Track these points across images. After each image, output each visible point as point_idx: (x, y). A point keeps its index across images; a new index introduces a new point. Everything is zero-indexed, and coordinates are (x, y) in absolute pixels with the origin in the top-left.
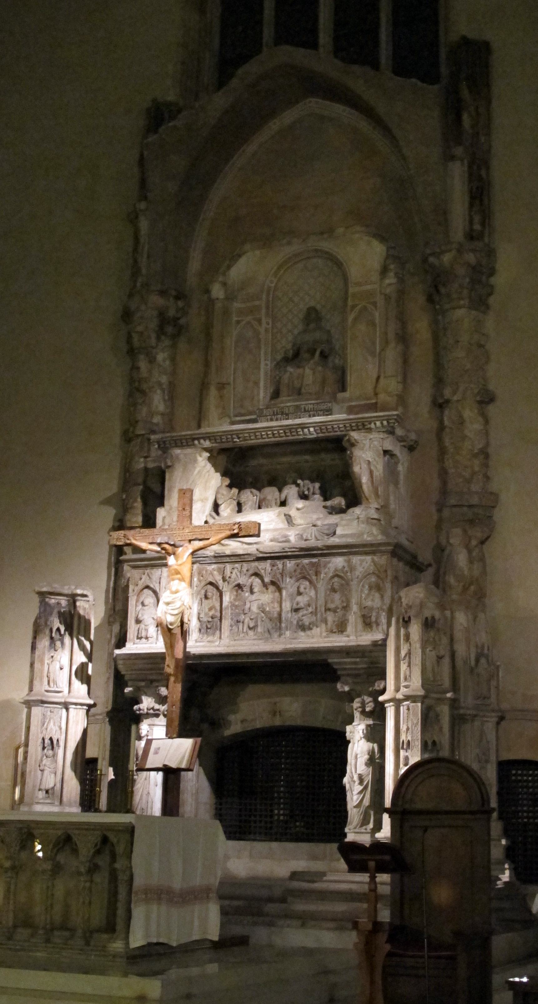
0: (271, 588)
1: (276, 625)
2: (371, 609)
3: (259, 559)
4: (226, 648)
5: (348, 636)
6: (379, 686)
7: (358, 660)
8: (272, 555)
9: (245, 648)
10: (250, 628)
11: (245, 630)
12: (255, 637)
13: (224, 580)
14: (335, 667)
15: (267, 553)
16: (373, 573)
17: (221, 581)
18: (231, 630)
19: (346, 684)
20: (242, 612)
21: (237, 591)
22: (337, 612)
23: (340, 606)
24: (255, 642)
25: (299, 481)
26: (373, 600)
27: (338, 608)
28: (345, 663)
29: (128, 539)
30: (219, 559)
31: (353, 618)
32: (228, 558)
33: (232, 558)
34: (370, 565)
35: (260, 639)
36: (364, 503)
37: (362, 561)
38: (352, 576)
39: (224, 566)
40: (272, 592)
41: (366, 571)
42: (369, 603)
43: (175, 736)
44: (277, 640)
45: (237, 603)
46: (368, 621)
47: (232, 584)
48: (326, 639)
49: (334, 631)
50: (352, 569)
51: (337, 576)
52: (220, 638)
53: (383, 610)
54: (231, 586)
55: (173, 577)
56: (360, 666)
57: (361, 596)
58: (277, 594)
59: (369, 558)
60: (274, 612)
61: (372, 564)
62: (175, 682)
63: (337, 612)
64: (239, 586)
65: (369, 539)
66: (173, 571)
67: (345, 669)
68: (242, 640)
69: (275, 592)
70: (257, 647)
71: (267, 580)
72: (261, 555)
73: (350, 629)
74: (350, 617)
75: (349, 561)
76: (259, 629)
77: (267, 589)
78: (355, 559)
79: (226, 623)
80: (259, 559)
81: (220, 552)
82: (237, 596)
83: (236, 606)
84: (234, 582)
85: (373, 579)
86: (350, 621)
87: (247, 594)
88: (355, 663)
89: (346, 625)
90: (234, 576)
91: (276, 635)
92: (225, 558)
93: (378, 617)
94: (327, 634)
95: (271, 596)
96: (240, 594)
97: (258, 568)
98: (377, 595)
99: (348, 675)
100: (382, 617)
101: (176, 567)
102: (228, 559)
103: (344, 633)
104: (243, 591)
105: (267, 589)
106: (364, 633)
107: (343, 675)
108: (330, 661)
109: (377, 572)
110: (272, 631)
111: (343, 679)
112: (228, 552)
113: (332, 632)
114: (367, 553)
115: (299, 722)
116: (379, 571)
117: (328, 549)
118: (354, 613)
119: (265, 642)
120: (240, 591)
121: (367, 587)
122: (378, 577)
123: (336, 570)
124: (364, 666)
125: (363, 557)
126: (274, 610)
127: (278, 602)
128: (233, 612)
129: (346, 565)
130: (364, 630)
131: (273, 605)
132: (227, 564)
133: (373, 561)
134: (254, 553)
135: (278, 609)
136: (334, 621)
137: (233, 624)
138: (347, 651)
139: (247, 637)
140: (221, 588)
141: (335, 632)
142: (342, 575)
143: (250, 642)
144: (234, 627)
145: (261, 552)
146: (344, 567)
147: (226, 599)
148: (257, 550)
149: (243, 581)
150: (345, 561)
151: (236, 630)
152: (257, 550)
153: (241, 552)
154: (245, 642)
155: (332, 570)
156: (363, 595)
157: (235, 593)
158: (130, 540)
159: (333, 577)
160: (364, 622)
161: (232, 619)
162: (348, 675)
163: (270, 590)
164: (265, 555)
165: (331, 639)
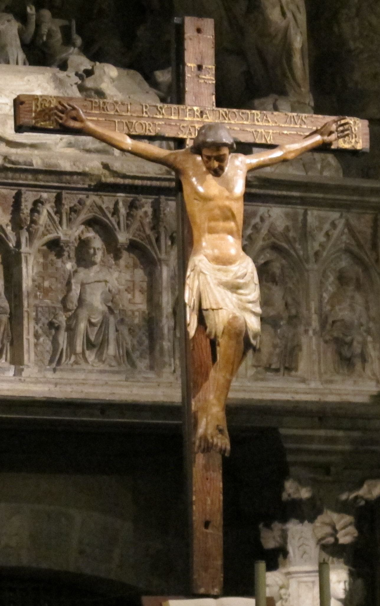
0: (126, 258)
1: (140, 343)
2: (347, 327)
3: (102, 187)
4: (52, 387)
5: (303, 381)
6: (370, 491)
7: (341, 434)
8: (138, 182)
9: (69, 389)
10: (89, 344)
11: (79, 349)
12: (102, 367)
13: (17, 224)
14: (289, 445)
15: (125, 176)
16: (348, 251)
17: (9, 228)
18: (36, 345)
19: (301, 482)
20: (59, 305)
21: (45, 256)
22: (280, 326)
23: (285, 315)
24: (105, 378)
25: (31, 10)
26: (352, 308)
27: (282, 319)
28: (311, 439)
29: (75, 119)
30: (10, 175)
31: (310, 344)
32: (30, 177)
33: (41, 177)
34: (342, 233)
35: (118, 372)
36: (291, 93)
37: (322, 220)
38: (305, 249)
39: (14, 192)
40: (127, 267)
41: (334, 245)
42: (343, 312)
43: (216, 591)
44: (151, 375)
45: (46, 284)
46: (346, 353)
47: (40, 238)
48: (261, 384)
49: (273, 367)
50: (305, 234)
51: (275, 247)
52: (17, 361)
53: (368, 332)
54: (38, 243)
55: (213, 224)
56: (339, 447)
57: (321, 296)
58: (140, 274)
59: (334, 215)
60: (133, 312)
61: (346, 230)
62: (206, 468)
63: (280, 326)
64: (55, 246)
65: (326, 173)
66: (217, 212)
67: (309, 452)
68: (73, 371)
69: (135, 266)
70: (125, 391)
71: (123, 237)
72: (111, 180)
73: (303, 365)
74: (304, 340)
75: (292, 217)
76: (111, 349)
77: (117, 257)
78: (313, 215)
79: (29, 328)
80: (102, 187)
81: (21, 160)
82: (45, 266)
83: (46, 292)
84: (44, 235)
85: (344, 263)
86: (305, 348)
87: (69, 266)
88: (332, 440)
89: (297, 355)
90: (43, 218)
91: (143, 364)
92: (23, 176)
93: (364, 344)
94: (258, 372)
95: (127, 276)
96: (52, 263)
97: (100, 208)
98: (359, 298)
99: (305, 465)
100: (370, 346)
101: (227, 203)
102: (30, 180)
103: (293, 373)
104: (59, 255)
105: (117, 257)
106: (337, 378)
107: (295, 464)
108: (283, 431)
109: (356, 249)
110: (135, 356)
111: (293, 470)
112: (37, 164)
113: (268, 368)
114: (333, 205)
115: (26, 559)
116: (360, 246)
117: (259, 187)
118: (315, 332)
119: (127, 380)
120: (52, 257)
121: (332, 279)
122: (357, 259)
123: (271, 233)
124: (347, 447)
125: (323, 213)
126: (134, 308)
127: (141, 291)
128: (37, 302)
129: (289, 223)
130: (338, 373)
131: (130, 296)
132: (23, 189)
133: (348, 225)
134: (96, 172)
135: (144, 307)
136: (275, 346)
137: (40, 331)
138: (322, 415)
139: (84, 365)
140: (12, 244)
141: (277, 370)
142: (285, 245)
143: (94, 377)
144: (41, 339)
145: (115, 174)
146: (287, 229)
147: (29, 272)
148: (106, 166)
149: (66, 235)
150: (287, 215)
151: (49, 346)
152: (106, 166)
153: (67, 166)
154: (81, 376)
155: (264, 231)
156: (325, 295)
157: (41, 260)
158: (82, 121)
159: (263, 249)
160: (340, 354)
161: (37, 320)
162: (305, 465)
163: (122, 262)
164: (120, 181)
165: (271, 384)
